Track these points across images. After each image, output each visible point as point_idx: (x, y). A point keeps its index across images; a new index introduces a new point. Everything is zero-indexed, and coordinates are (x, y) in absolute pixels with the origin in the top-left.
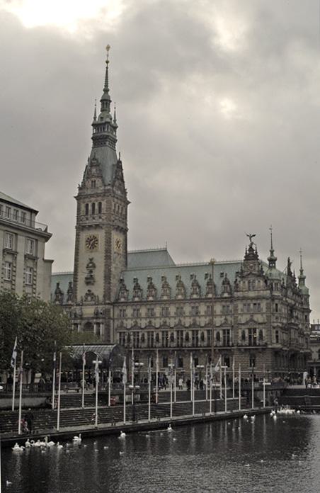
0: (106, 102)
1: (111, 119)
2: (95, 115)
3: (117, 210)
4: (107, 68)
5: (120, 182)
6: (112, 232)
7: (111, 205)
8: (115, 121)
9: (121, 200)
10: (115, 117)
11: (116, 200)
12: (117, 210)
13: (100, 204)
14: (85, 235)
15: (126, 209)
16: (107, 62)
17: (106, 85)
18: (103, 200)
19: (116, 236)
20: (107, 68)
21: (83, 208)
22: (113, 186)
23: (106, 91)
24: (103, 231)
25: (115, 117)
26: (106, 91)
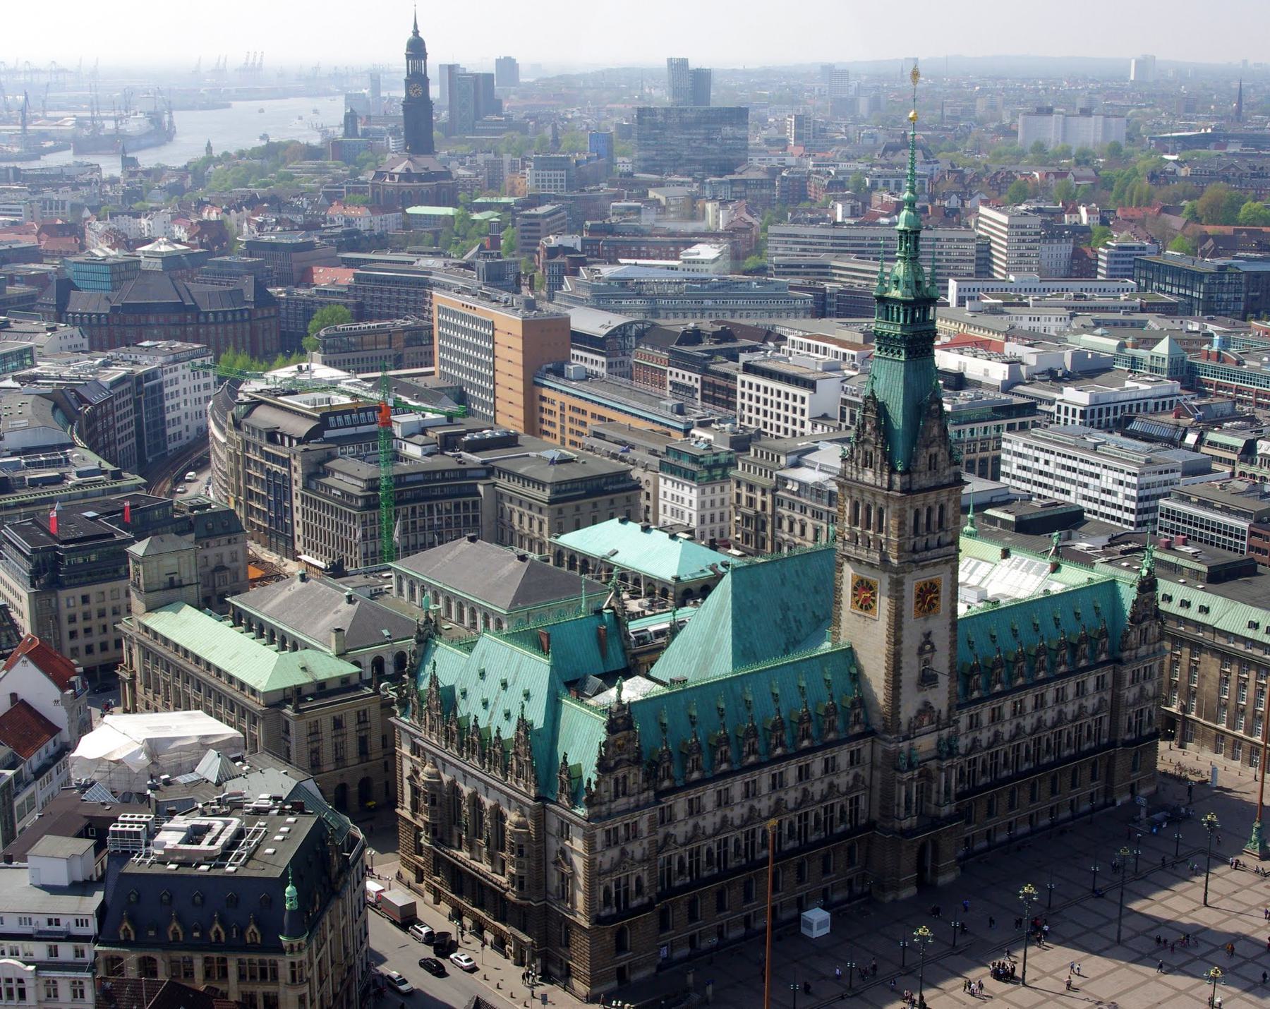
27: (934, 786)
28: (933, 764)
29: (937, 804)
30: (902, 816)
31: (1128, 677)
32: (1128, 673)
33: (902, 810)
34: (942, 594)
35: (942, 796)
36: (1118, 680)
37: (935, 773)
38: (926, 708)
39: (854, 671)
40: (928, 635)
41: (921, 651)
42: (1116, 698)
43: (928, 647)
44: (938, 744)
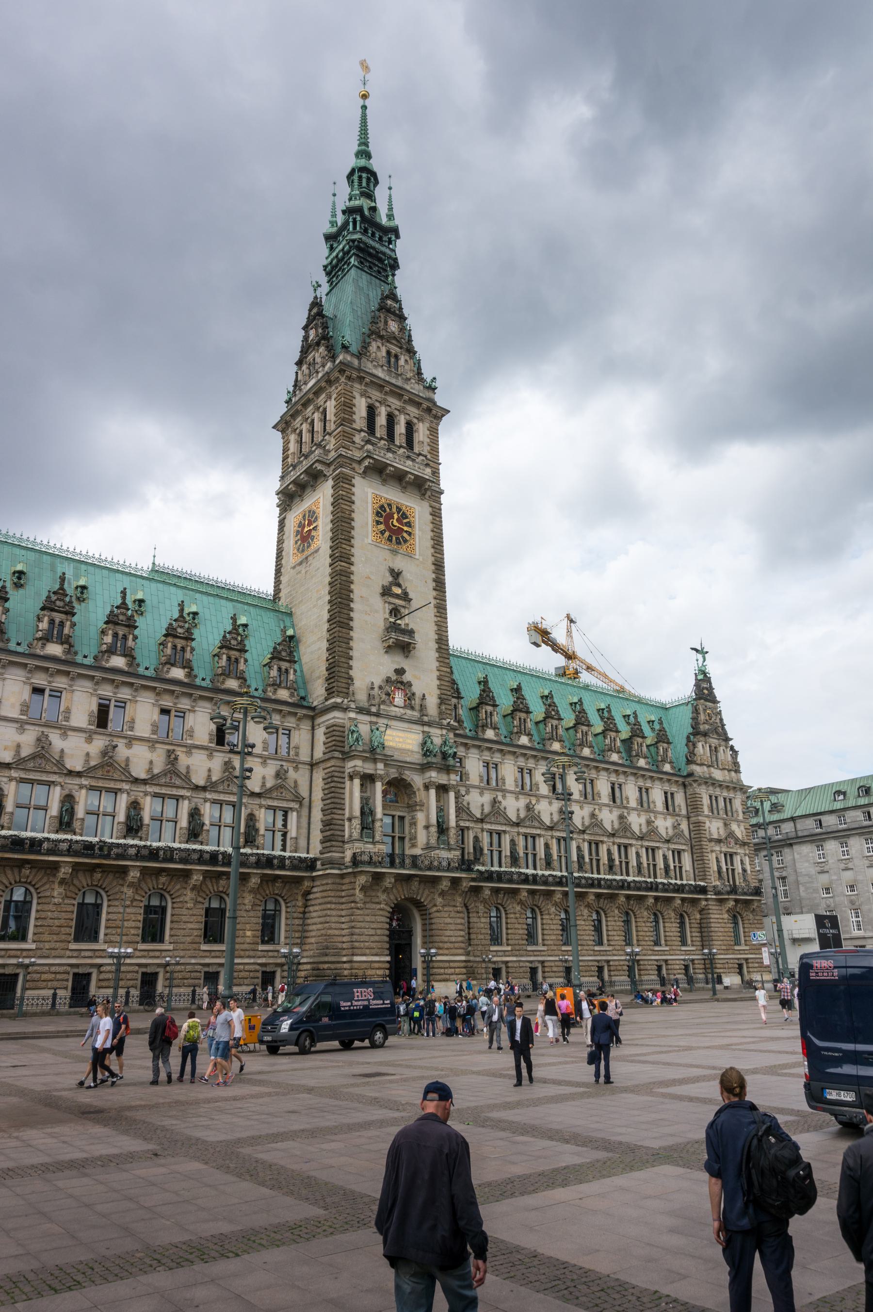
0: (364, 178)
1: (374, 209)
2: (334, 215)
3: (381, 420)
4: (364, 107)
5: (395, 349)
6: (358, 481)
7: (351, 406)
8: (390, 217)
9: (400, 396)
10: (391, 209)
11: (376, 394)
12: (381, 420)
13: (325, 410)
14: (294, 518)
15: (434, 433)
16: (365, 97)
17: (364, 141)
18: (329, 397)
19: (367, 494)
20: (364, 107)
21: (293, 447)
22: (359, 356)
23: (364, 153)
24: (330, 483)
25: (391, 209)
26: (364, 153)
27: (420, 817)
28: (417, 780)
29: (428, 847)
30: (356, 834)
31: (706, 801)
32: (704, 794)
33: (356, 823)
34: (417, 532)
35: (433, 829)
36: (694, 806)
37: (421, 795)
38: (398, 680)
39: (290, 632)
40: (396, 575)
41: (386, 592)
42: (697, 828)
43: (397, 591)
44: (424, 743)
